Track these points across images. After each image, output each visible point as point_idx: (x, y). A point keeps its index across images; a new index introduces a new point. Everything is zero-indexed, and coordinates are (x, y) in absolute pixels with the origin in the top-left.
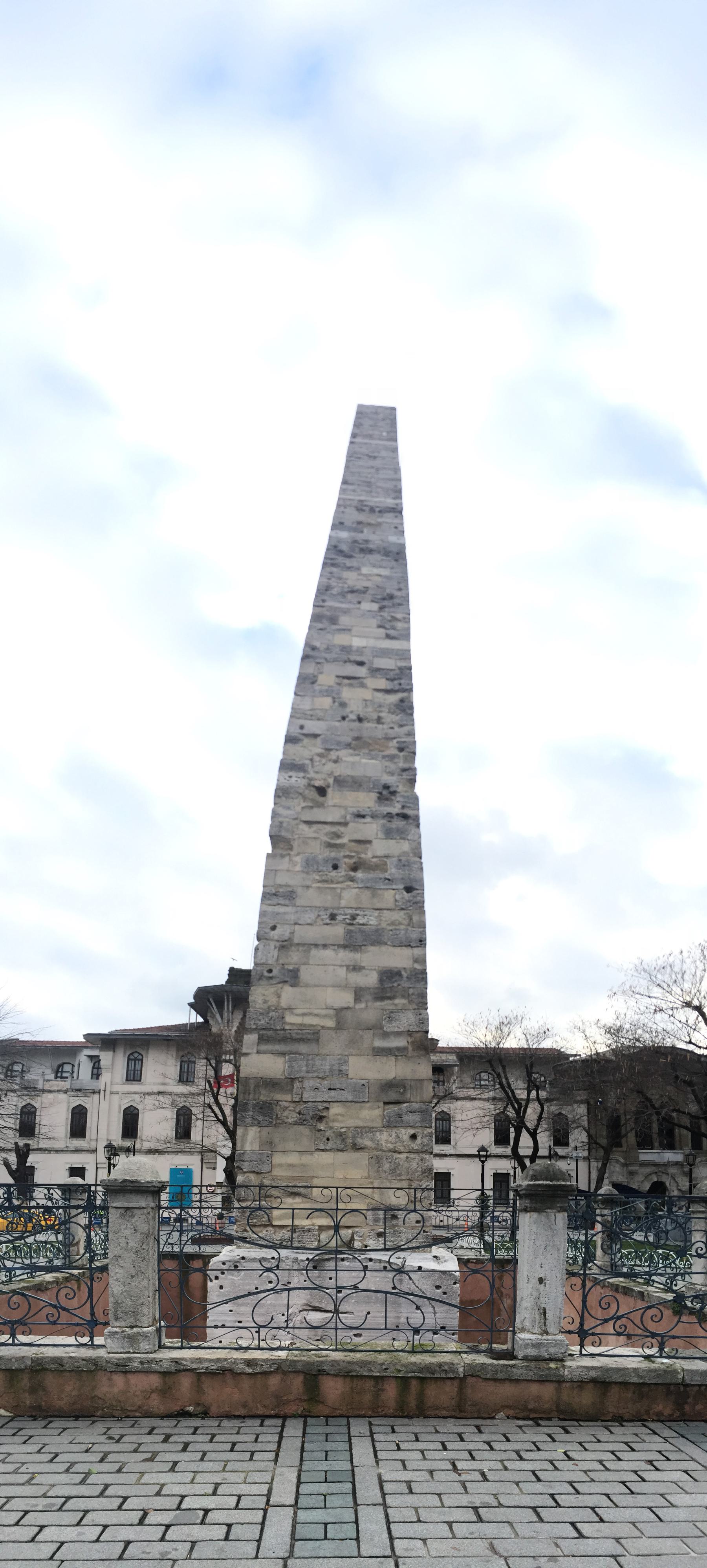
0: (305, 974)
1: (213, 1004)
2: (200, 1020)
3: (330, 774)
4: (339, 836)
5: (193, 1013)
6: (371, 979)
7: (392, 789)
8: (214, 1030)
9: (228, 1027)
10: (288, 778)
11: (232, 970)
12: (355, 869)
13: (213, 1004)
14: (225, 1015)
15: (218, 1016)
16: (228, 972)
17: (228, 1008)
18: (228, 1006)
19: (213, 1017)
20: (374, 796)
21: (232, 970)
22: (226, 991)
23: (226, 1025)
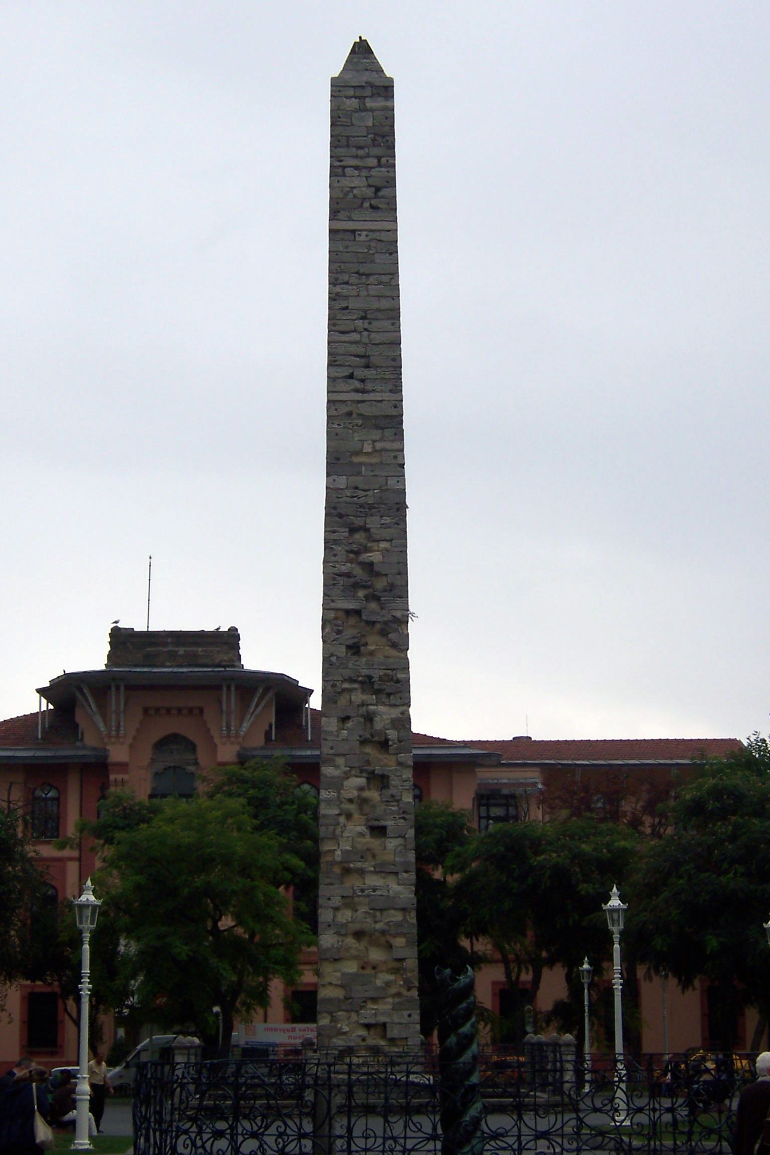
1: (90, 699)
2: (51, 707)
5: (44, 701)
7: (396, 798)
8: (90, 740)
9: (117, 737)
10: (328, 793)
13: (90, 699)
15: (98, 719)
18: (115, 701)
22: (114, 679)
23: (114, 733)
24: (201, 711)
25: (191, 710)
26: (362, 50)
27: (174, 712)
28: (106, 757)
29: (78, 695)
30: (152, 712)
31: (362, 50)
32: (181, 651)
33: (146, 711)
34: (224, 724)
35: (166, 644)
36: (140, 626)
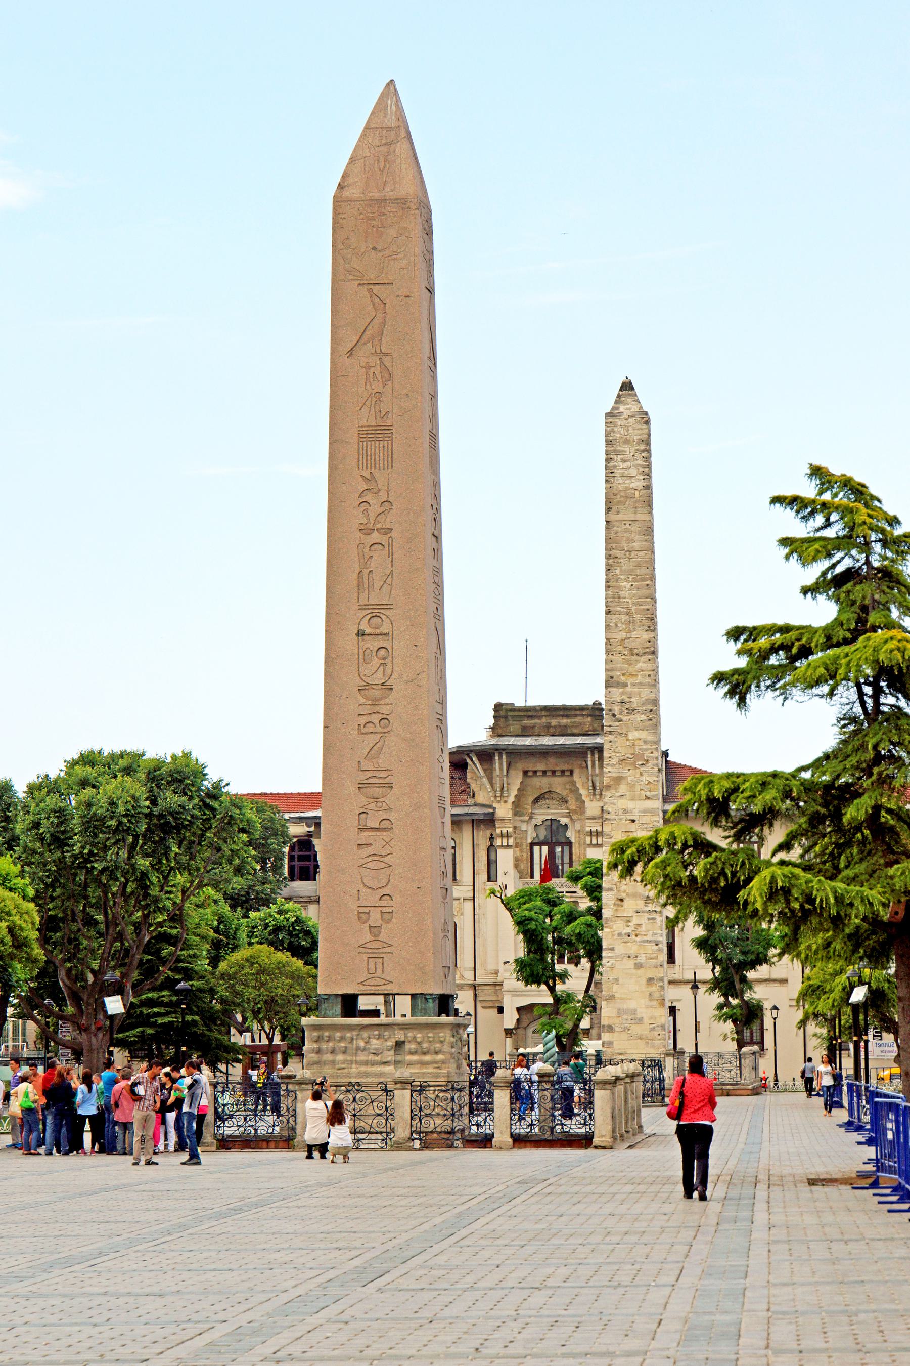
0: (621, 981)
3: (625, 891)
4: (629, 921)
6: (644, 981)
8: (481, 798)
9: (501, 796)
11: (498, 707)
12: (636, 936)
13: (478, 765)
14: (497, 782)
15: (485, 781)
16: (493, 713)
17: (501, 769)
18: (499, 764)
19: (477, 778)
20: (643, 902)
21: (498, 707)
22: (497, 750)
23: (499, 794)
24: (572, 772)
25: (563, 772)
26: (627, 387)
27: (549, 773)
28: (493, 814)
29: (468, 761)
30: (530, 774)
31: (627, 387)
32: (554, 722)
33: (525, 773)
34: (591, 784)
35: (540, 717)
36: (519, 703)
